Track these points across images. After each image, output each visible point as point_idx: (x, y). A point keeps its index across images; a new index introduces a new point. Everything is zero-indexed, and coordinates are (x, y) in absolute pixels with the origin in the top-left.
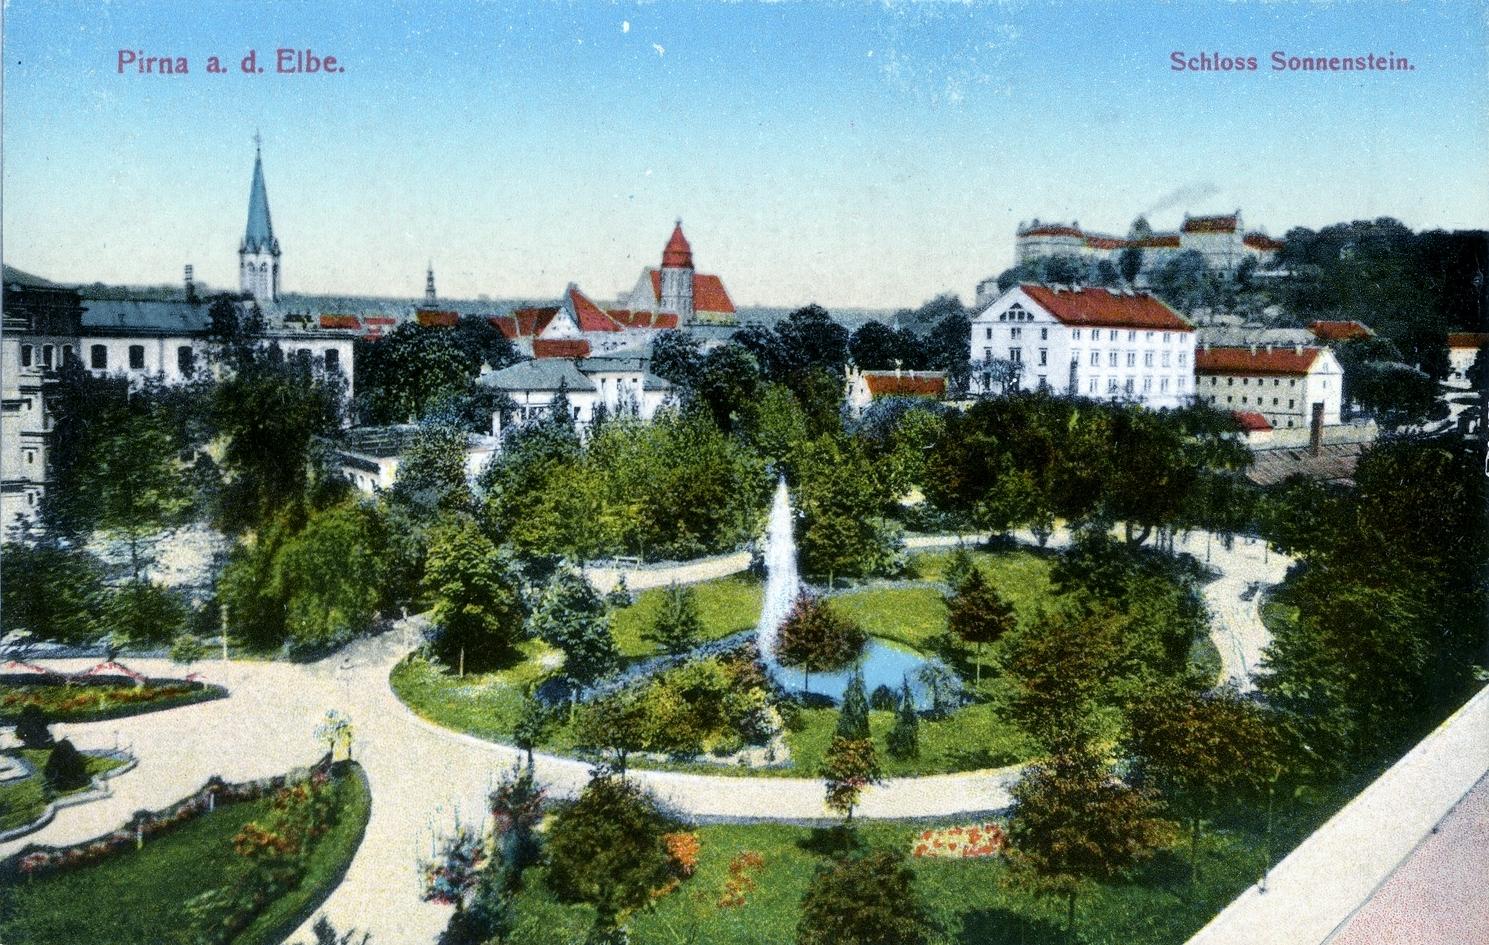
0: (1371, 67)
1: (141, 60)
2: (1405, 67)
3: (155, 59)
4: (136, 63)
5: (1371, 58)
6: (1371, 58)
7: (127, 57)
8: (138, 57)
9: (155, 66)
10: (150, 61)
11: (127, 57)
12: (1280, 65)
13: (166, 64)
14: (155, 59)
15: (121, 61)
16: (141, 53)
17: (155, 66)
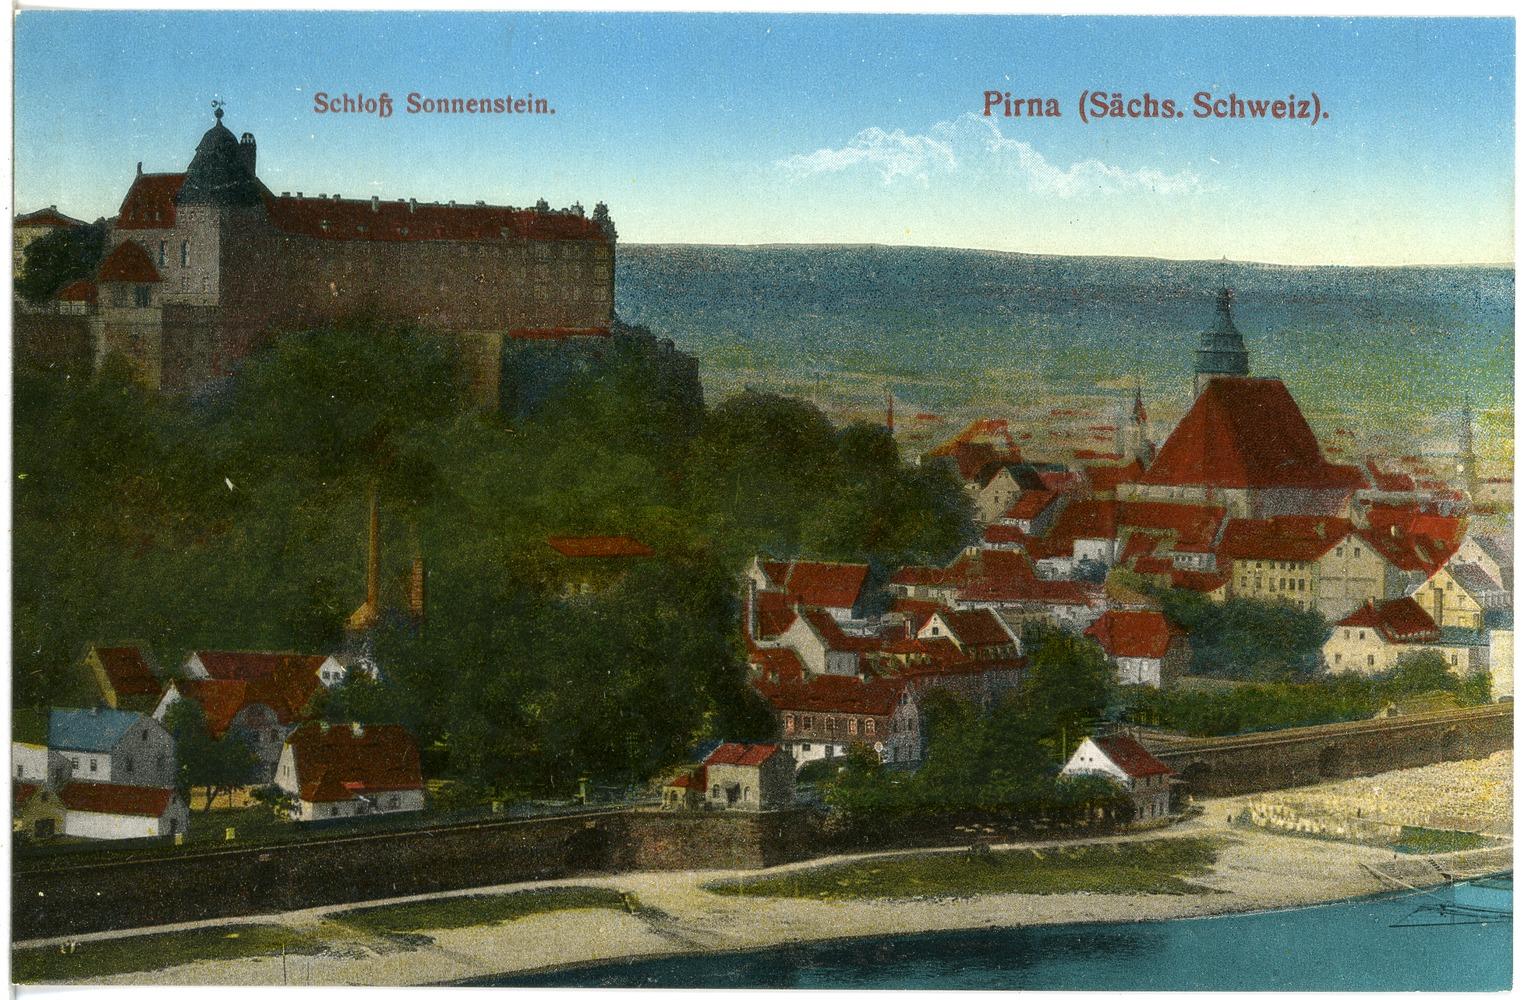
0: (510, 111)
1: (1008, 104)
2: (545, 110)
3: (1022, 101)
4: (1002, 107)
5: (509, 100)
6: (509, 100)
7: (993, 98)
8: (1005, 98)
9: (1024, 108)
10: (1018, 103)
11: (993, 98)
12: (322, 107)
13: (1035, 105)
14: (1022, 101)
15: (988, 104)
16: (1008, 95)
17: (1024, 108)
